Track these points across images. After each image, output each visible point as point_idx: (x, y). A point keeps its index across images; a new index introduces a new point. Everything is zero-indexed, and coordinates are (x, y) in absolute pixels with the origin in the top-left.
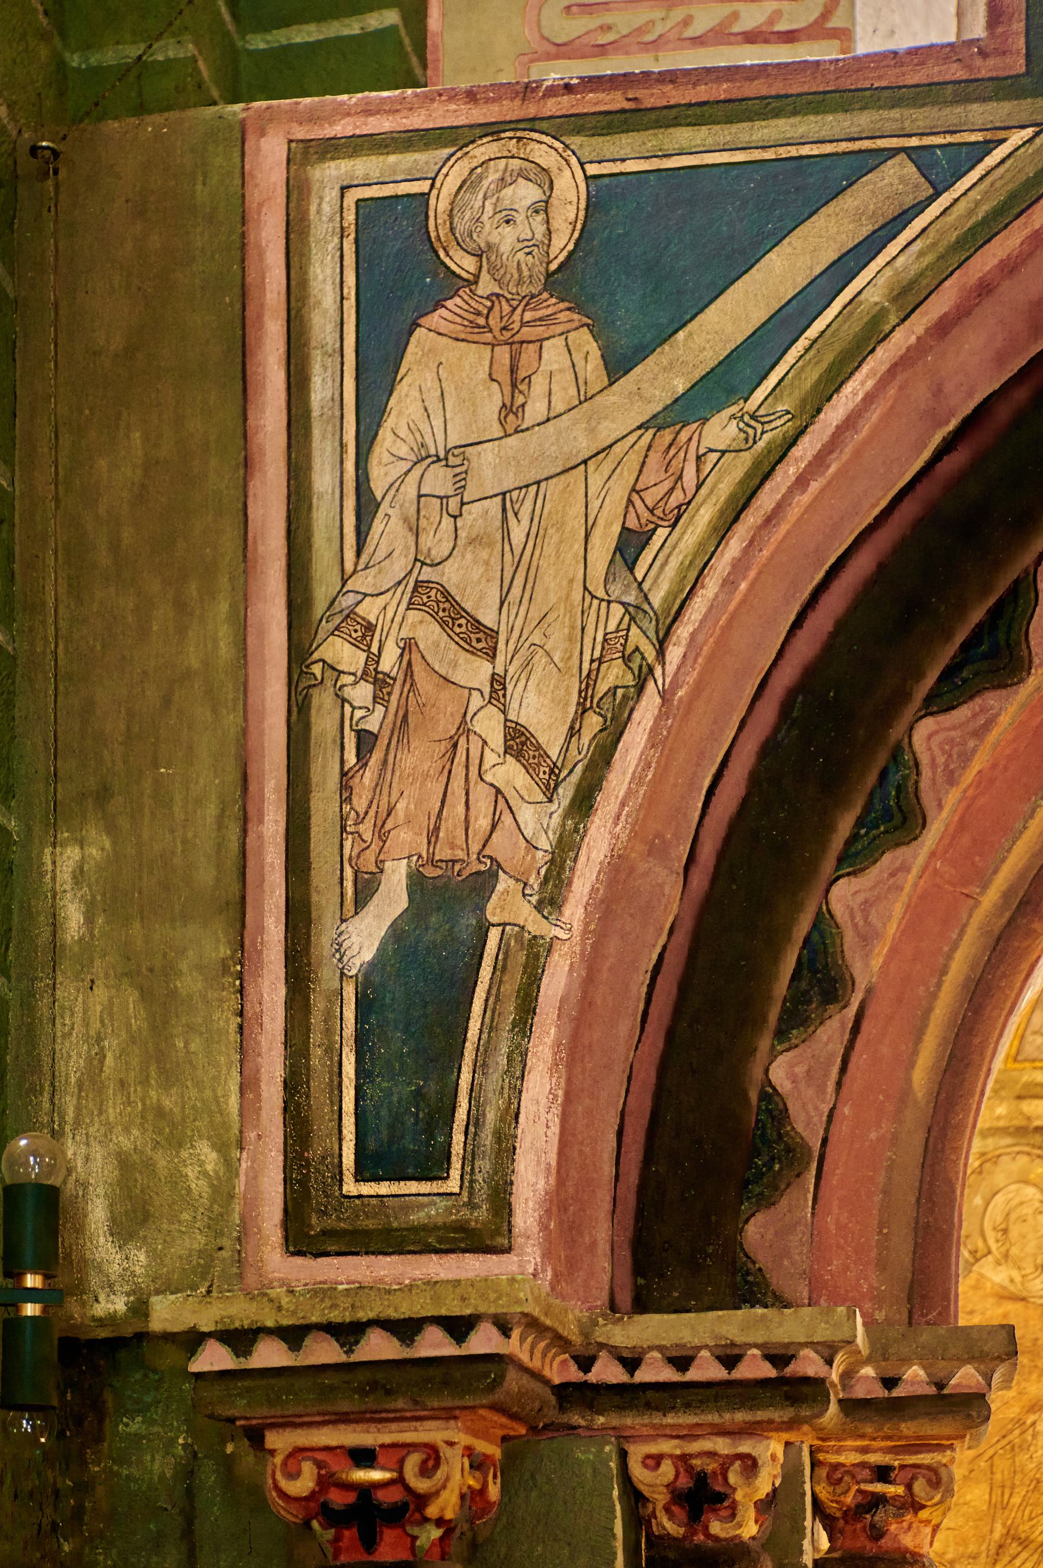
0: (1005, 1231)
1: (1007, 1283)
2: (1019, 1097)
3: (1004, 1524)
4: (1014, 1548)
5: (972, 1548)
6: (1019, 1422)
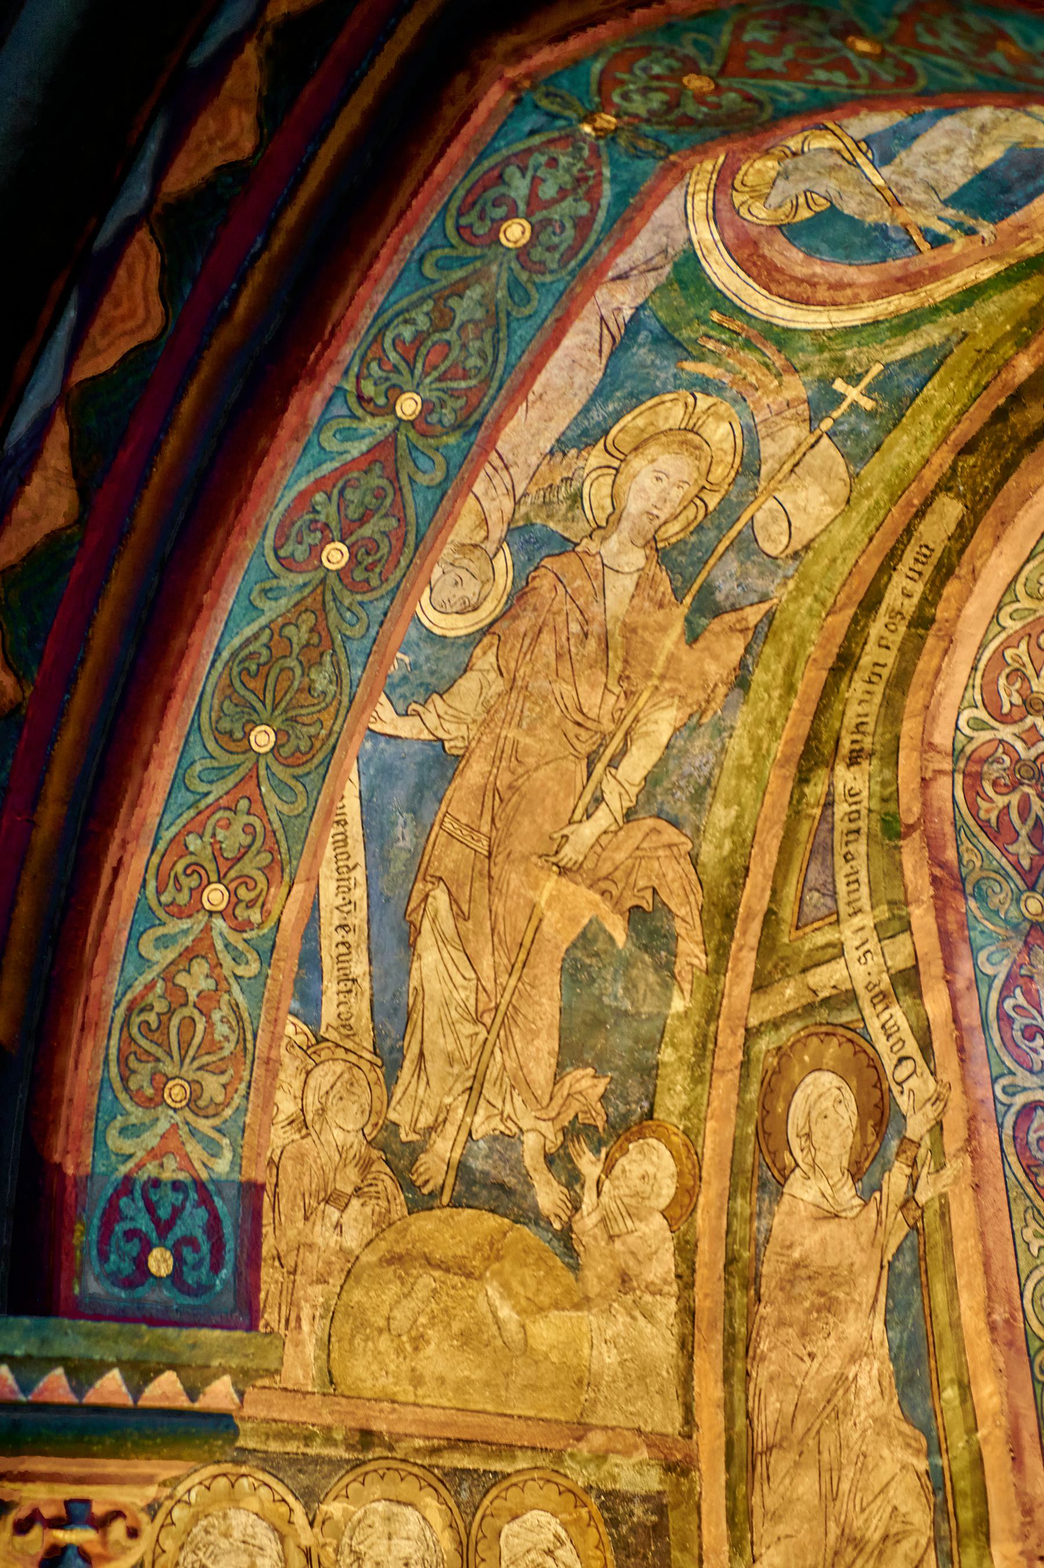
0: (808, 1136)
1: (820, 1200)
2: (804, 971)
4: (850, 1553)
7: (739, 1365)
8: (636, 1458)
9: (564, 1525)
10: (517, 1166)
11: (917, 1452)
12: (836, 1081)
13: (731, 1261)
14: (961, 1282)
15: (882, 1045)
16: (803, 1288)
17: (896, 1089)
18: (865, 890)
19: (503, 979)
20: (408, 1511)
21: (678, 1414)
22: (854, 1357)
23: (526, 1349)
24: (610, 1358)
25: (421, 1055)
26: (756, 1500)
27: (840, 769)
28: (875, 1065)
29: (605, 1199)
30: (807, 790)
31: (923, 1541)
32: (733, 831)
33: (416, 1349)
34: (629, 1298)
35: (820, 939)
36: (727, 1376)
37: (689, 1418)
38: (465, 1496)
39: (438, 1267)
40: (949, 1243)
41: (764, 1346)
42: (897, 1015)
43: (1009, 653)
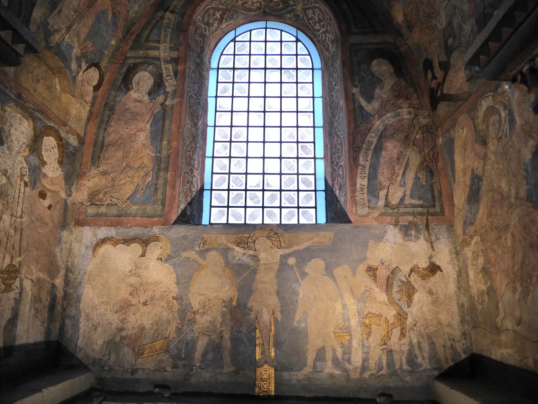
0: (138, 84)
1: (137, 97)
3: (126, 162)
5: (116, 169)
6: (135, 134)
7: (103, 126)
8: (74, 137)
9: (57, 143)
10: (70, 54)
11: (153, 152)
12: (149, 75)
13: (106, 104)
14: (174, 122)
15: (164, 71)
16: (127, 114)
17: (165, 81)
18: (168, 39)
19: (85, 7)
20: (26, 120)
21: (83, 132)
22: (140, 130)
23: (59, 100)
24: (74, 112)
25: (61, 10)
26: (102, 155)
27: (168, 13)
28: (161, 74)
29: (84, 76)
30: (158, 13)
31: (150, 169)
32: (137, 12)
33: (37, 82)
34: (82, 101)
35: (153, 44)
36: (99, 128)
37: (85, 134)
38: (38, 125)
39: (47, 66)
40: (173, 114)
41: (112, 124)
42: (170, 66)
43: (210, 10)
